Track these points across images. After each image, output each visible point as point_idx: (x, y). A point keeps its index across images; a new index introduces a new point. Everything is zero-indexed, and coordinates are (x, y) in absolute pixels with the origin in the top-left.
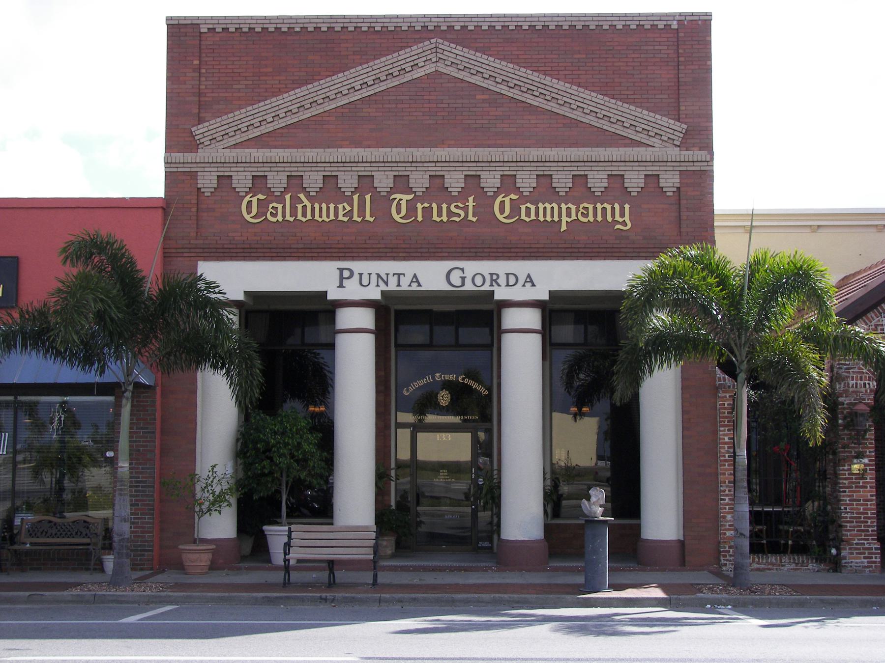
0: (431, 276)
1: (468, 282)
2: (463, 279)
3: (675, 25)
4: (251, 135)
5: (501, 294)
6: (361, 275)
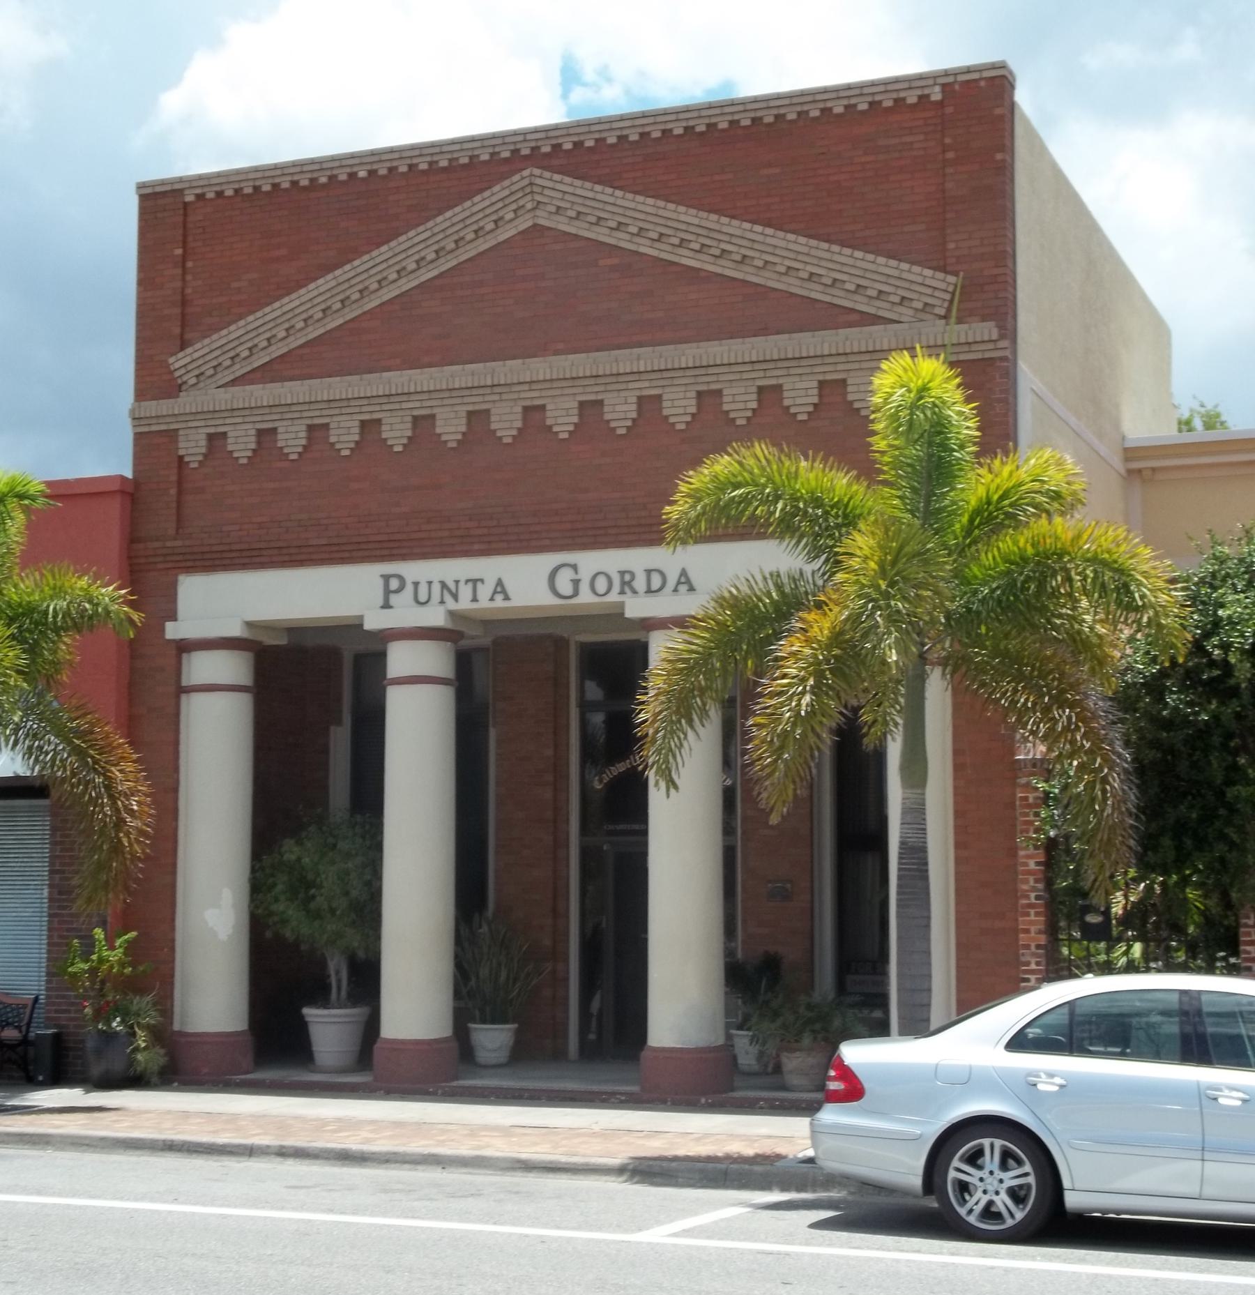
0: (525, 583)
1: (584, 587)
2: (576, 583)
3: (936, 94)
4: (261, 359)
5: (636, 608)
6: (416, 584)
